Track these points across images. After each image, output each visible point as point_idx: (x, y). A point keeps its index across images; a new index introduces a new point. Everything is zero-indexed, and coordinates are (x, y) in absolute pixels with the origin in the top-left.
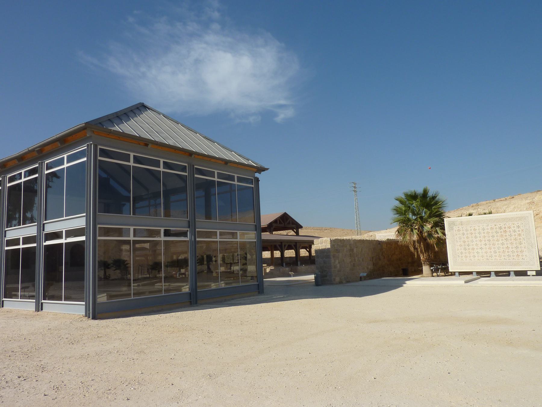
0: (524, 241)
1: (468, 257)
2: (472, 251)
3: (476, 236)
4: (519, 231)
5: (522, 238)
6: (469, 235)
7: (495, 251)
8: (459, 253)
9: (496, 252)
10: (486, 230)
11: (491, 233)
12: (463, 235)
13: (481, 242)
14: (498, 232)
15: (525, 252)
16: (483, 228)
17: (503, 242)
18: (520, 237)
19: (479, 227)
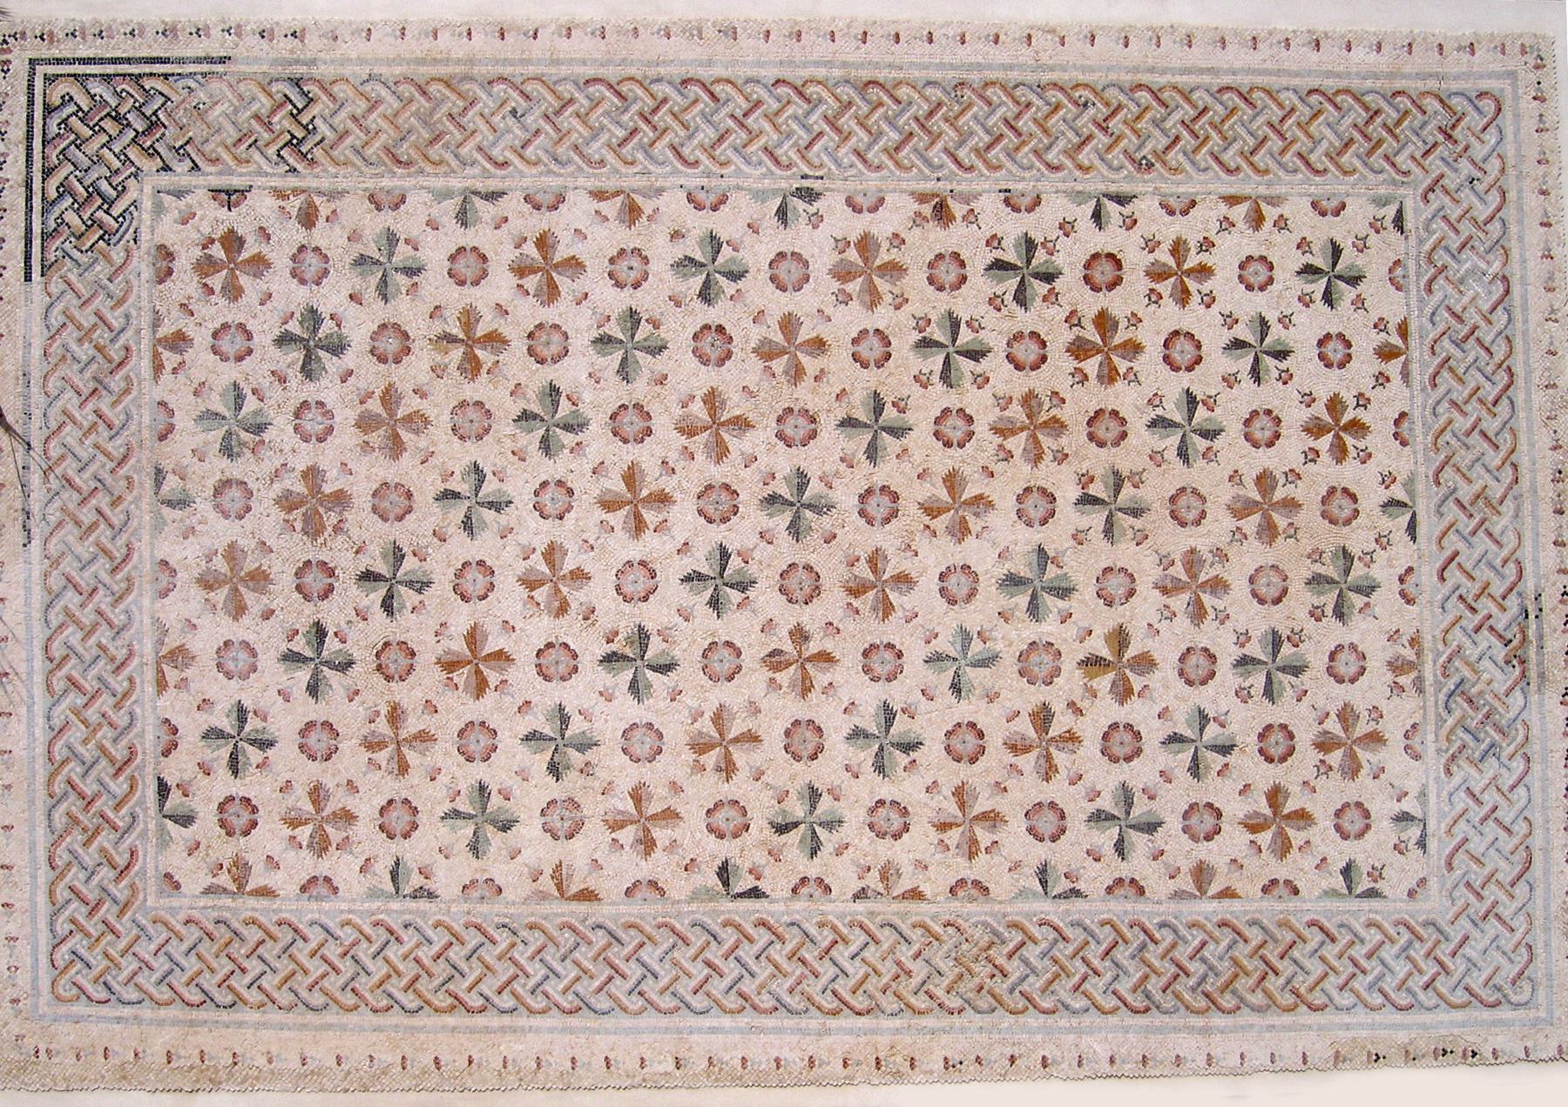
0: (1403, 552)
1: (365, 830)
2: (460, 708)
3: (554, 391)
5: (1372, 496)
6: (418, 367)
7: (889, 715)
9: (908, 747)
10: (758, 289)
11: (838, 360)
12: (308, 370)
14: (975, 355)
15: (1392, 756)
16: (714, 243)
17: (1055, 537)
18: (1349, 473)
19: (632, 213)
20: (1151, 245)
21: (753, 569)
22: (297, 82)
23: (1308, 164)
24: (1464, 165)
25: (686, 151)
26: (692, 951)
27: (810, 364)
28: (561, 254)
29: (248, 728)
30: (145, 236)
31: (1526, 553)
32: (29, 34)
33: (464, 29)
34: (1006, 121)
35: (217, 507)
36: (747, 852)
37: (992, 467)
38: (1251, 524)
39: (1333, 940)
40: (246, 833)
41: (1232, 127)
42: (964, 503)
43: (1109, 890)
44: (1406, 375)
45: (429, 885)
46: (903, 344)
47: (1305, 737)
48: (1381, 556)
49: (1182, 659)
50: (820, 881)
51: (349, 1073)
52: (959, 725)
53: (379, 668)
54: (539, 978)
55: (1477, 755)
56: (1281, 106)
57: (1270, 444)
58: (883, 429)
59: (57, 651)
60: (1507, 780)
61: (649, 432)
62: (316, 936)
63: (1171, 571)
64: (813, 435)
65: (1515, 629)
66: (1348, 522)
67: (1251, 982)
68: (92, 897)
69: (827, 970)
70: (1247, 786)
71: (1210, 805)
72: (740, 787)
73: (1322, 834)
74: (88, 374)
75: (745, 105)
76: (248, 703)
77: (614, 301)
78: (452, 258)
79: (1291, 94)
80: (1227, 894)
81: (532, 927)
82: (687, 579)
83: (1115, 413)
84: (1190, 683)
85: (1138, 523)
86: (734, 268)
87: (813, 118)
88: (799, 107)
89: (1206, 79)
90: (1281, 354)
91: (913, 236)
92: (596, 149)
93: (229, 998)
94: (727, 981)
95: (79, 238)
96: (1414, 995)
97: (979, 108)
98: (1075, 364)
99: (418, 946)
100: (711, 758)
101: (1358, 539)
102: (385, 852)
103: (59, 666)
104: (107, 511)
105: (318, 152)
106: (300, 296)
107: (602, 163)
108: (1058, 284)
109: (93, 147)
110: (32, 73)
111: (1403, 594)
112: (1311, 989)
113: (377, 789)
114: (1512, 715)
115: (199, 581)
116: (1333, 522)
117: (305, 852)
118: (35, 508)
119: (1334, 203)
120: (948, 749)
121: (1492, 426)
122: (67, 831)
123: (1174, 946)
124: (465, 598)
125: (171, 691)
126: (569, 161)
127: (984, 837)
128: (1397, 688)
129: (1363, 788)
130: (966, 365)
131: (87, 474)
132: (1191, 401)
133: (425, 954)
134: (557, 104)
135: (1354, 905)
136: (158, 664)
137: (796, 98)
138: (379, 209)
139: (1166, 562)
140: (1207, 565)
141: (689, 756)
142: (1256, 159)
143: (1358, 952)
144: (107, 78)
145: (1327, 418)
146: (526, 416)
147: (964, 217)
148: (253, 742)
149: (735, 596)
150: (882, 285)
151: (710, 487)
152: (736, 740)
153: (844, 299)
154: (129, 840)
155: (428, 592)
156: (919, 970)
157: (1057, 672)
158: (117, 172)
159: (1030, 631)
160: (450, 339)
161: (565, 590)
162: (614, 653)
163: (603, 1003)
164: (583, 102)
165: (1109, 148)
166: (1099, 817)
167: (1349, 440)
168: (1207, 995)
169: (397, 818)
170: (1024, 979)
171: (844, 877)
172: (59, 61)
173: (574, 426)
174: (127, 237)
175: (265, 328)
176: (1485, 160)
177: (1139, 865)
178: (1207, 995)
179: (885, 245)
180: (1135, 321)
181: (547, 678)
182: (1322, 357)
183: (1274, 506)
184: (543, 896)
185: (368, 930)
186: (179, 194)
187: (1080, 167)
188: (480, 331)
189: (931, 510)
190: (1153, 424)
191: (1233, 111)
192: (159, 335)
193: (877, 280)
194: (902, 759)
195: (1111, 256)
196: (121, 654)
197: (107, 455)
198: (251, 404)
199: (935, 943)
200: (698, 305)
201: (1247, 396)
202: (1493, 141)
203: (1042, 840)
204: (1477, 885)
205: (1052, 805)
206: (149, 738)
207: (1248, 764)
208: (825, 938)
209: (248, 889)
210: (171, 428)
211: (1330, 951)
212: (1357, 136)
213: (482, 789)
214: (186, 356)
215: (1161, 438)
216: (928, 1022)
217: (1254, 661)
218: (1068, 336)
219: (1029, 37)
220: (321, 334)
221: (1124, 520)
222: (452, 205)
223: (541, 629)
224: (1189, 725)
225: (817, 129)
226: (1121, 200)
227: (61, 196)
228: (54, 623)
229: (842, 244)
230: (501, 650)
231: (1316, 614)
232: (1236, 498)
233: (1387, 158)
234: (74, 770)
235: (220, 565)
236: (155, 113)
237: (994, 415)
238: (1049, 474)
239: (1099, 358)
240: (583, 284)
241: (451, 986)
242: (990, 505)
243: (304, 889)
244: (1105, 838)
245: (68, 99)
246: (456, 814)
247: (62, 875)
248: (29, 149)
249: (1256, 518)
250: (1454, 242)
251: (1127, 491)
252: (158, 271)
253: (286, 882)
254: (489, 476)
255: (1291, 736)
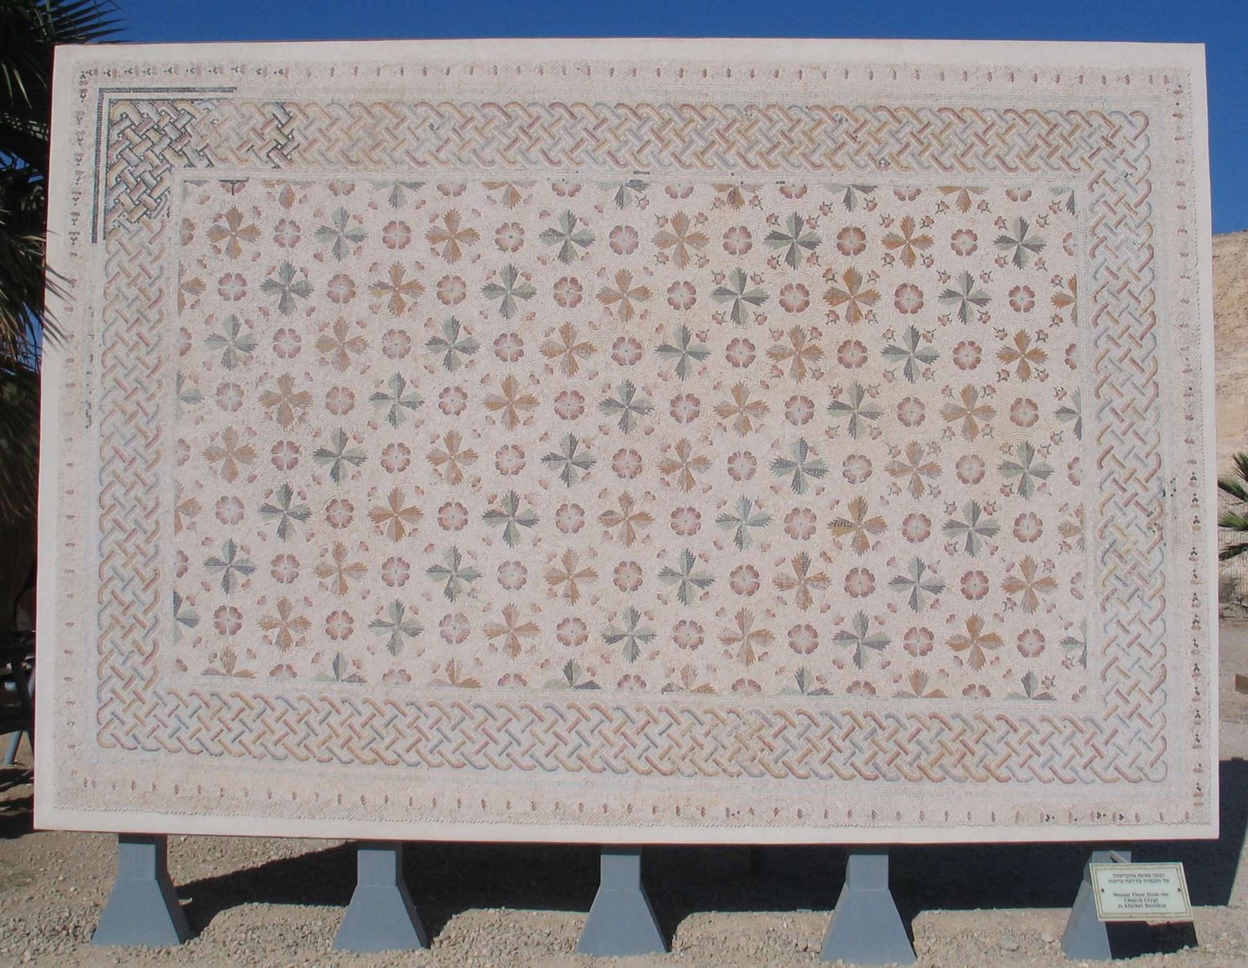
0: (1071, 447)
1: (316, 632)
2: (385, 548)
3: (454, 325)
4: (1021, 299)
5: (1048, 406)
6: (359, 307)
7: (689, 559)
8: (196, 564)
9: (704, 582)
10: (601, 252)
11: (658, 306)
12: (284, 308)
13: (512, 421)
14: (757, 300)
15: (1061, 595)
16: (571, 220)
18: (1031, 388)
19: (512, 197)
20: (887, 222)
21: (593, 452)
22: (282, 106)
23: (1004, 163)
24: (1120, 164)
25: (552, 155)
26: (545, 726)
27: (638, 306)
28: (462, 226)
29: (236, 559)
30: (174, 212)
31: (1164, 449)
32: (100, 71)
33: (398, 69)
34: (783, 133)
35: (218, 402)
36: (585, 656)
37: (768, 381)
38: (958, 424)
39: (1015, 731)
40: (233, 633)
41: (948, 137)
42: (748, 407)
43: (849, 690)
44: (1074, 317)
45: (361, 674)
46: (705, 292)
47: (996, 580)
48: (1054, 449)
49: (906, 523)
50: (638, 678)
51: (301, 804)
52: (741, 568)
53: (328, 518)
54: (435, 741)
55: (1125, 596)
56: (984, 121)
57: (973, 367)
58: (690, 353)
59: (108, 501)
60: (1147, 616)
61: (521, 353)
62: (280, 706)
63: (899, 458)
64: (639, 357)
65: (1155, 504)
66: (1030, 424)
67: (953, 760)
68: (127, 674)
69: (642, 742)
70: (952, 616)
71: (924, 630)
72: (582, 609)
73: (1008, 654)
74: (134, 308)
75: (595, 122)
76: (236, 541)
77: (498, 260)
78: (386, 229)
79: (992, 113)
80: (937, 694)
81: (432, 705)
82: (546, 459)
83: (858, 343)
84: (911, 540)
85: (874, 423)
86: (584, 237)
87: (644, 130)
88: (634, 123)
89: (929, 103)
90: (982, 301)
91: (713, 215)
92: (489, 154)
93: (219, 749)
94: (570, 748)
95: (130, 212)
96: (1076, 772)
97: (763, 124)
98: (830, 308)
99: (352, 715)
100: (561, 588)
101: (1037, 436)
102: (330, 649)
103: (108, 512)
104: (144, 403)
105: (295, 155)
106: (281, 254)
107: (492, 162)
108: (818, 250)
109: (140, 150)
110: (101, 99)
111: (1071, 477)
112: (999, 766)
113: (327, 603)
114: (1152, 568)
115: (205, 454)
116: (1019, 424)
117: (274, 647)
118: (95, 402)
119: (1024, 191)
120: (733, 585)
121: (1137, 354)
122: (111, 627)
123: (896, 732)
124: (389, 470)
125: (185, 531)
126: (469, 161)
127: (758, 649)
128: (1065, 546)
129: (1039, 619)
130: (750, 308)
131: (132, 378)
132: (915, 335)
133: (357, 721)
134: (462, 121)
135: (1031, 704)
136: (176, 511)
137: (630, 116)
138: (336, 194)
139: (893, 451)
140: (925, 455)
141: (545, 585)
142: (966, 160)
143: (1035, 739)
144: (152, 102)
145: (1016, 348)
146: (435, 342)
147: (751, 202)
148: (240, 568)
149: (581, 472)
150: (690, 250)
151: (564, 393)
152: (579, 575)
153: (663, 259)
154: (153, 635)
155: (365, 464)
156: (709, 744)
157: (813, 530)
158: (157, 167)
159: (795, 500)
160: (383, 286)
161: (459, 465)
162: (493, 511)
163: (480, 760)
164: (480, 120)
165: (857, 152)
166: (842, 637)
167: (1032, 364)
168: (920, 768)
169: (340, 625)
170: (785, 752)
171: (655, 674)
172: (119, 90)
173: (469, 348)
174: (162, 213)
175: (255, 276)
176: (1136, 161)
177: (871, 671)
178: (920, 768)
179: (693, 222)
180: (874, 276)
181: (446, 528)
182: (1012, 303)
183: (976, 412)
184: (440, 683)
185: (317, 703)
186: (198, 183)
187: (836, 166)
188: (405, 280)
189: (723, 411)
190: (886, 352)
191: (949, 125)
192: (182, 282)
193: (687, 246)
194: (699, 591)
195: (857, 230)
196: (151, 504)
197: (145, 365)
198: (244, 330)
199: (721, 725)
200: (558, 262)
201: (956, 332)
202: (1143, 146)
203: (800, 652)
204: (1124, 691)
205: (808, 627)
206: (168, 564)
207: (953, 599)
208: (641, 718)
209: (234, 672)
210: (189, 347)
211: (1013, 739)
212: (1041, 143)
213: (398, 605)
214: (201, 296)
215: (893, 361)
216: (716, 782)
217: (959, 525)
218: (826, 287)
219: (801, 72)
220: (293, 282)
221: (864, 421)
222: (387, 192)
223: (443, 492)
224: (910, 571)
225: (646, 139)
226: (866, 189)
227: (118, 183)
228: (105, 483)
229: (661, 221)
230: (414, 508)
231: (1006, 491)
232: (947, 406)
233: (1063, 159)
234: (117, 585)
235: (221, 444)
236: (184, 127)
237: (770, 344)
238: (808, 387)
239: (847, 303)
240: (477, 248)
241: (373, 745)
242: (766, 409)
243: (272, 673)
244: (847, 652)
245: (125, 117)
246: (379, 623)
247: (106, 659)
248: (98, 151)
249: (962, 420)
250: (1112, 220)
251: (867, 399)
252: (183, 237)
253: (260, 667)
254: (408, 383)
255: (986, 580)
